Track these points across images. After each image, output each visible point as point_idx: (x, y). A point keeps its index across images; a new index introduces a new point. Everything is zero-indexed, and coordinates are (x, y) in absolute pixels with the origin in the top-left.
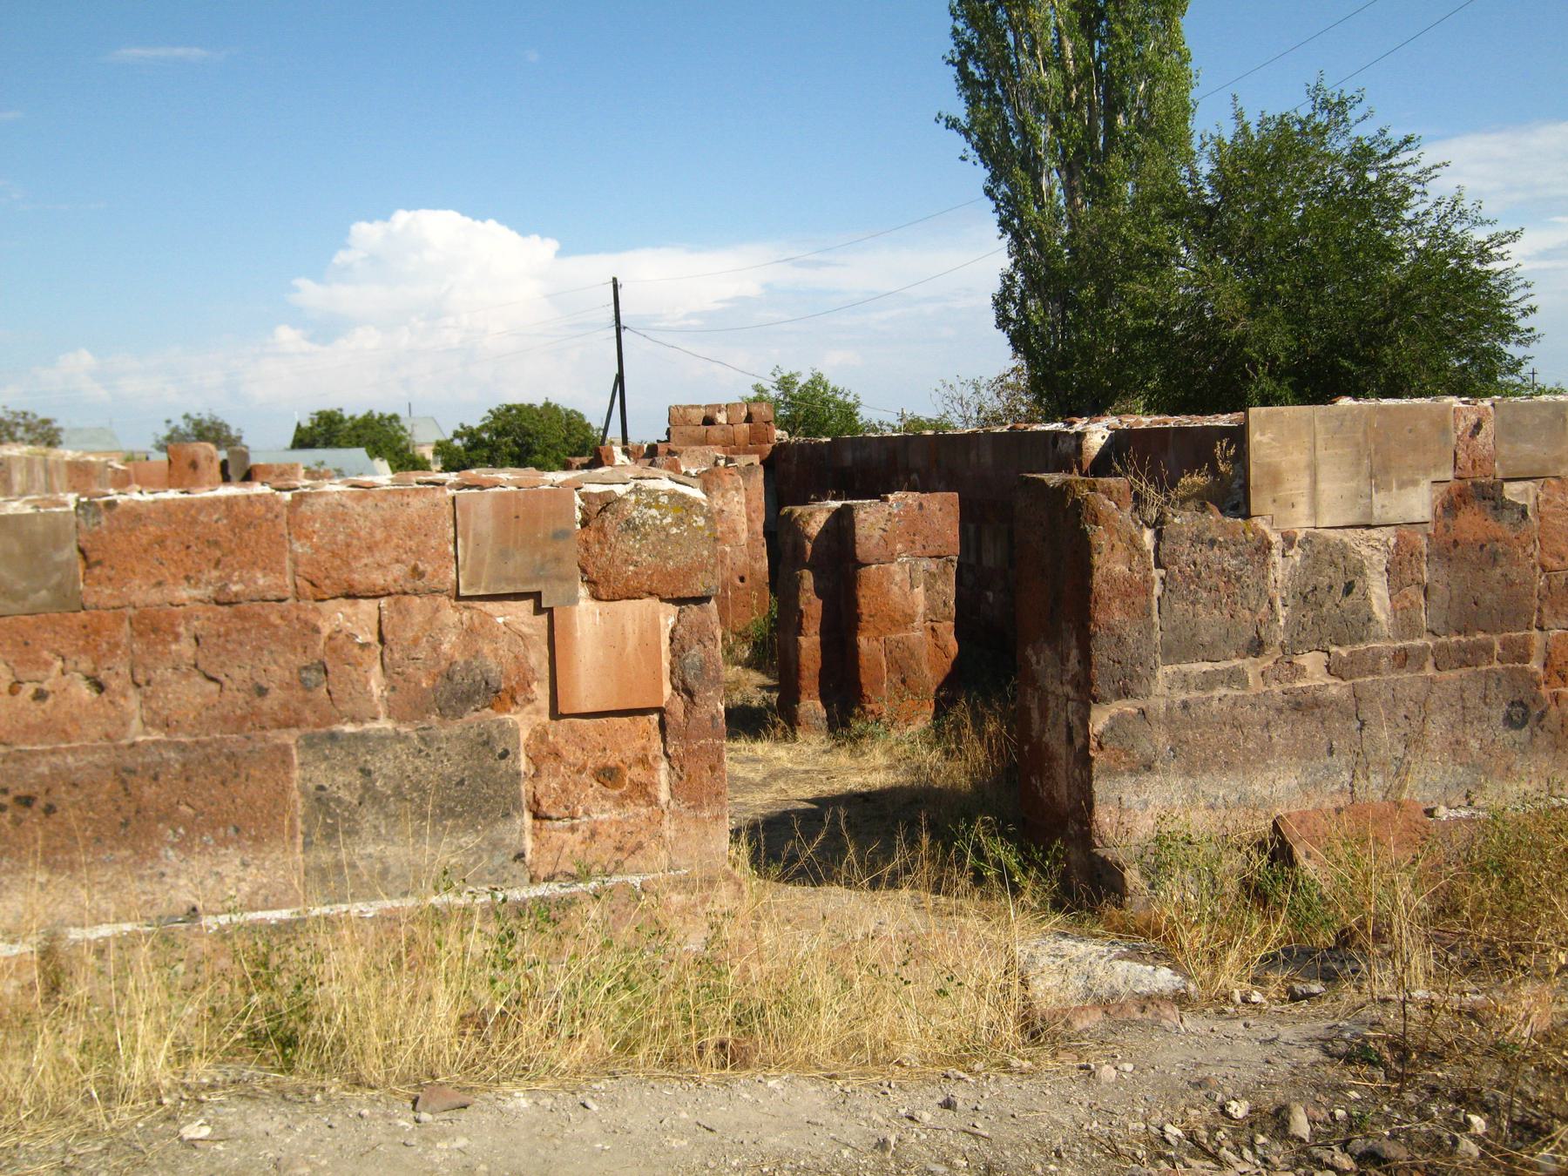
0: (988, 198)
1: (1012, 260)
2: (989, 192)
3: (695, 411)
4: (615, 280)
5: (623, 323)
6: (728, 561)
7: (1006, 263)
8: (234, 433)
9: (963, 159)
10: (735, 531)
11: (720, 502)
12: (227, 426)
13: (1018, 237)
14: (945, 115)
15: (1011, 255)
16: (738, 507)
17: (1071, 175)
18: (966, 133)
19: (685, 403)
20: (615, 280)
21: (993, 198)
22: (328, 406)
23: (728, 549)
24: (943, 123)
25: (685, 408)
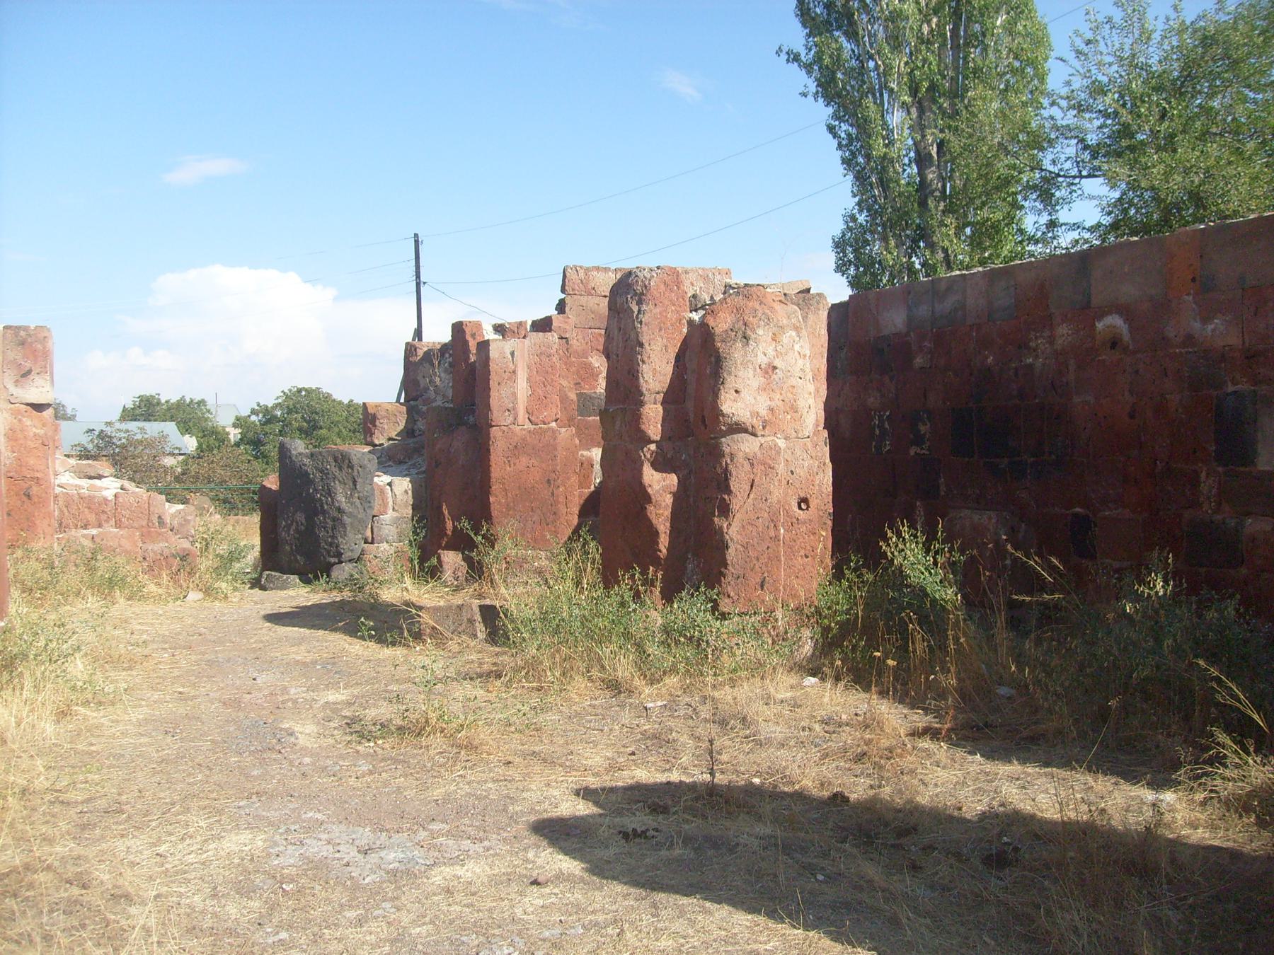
0: (831, 136)
1: (857, 199)
2: (831, 129)
3: (601, 275)
4: (416, 235)
5: (422, 279)
6: (781, 468)
7: (851, 203)
8: (69, 412)
9: (804, 95)
10: (794, 409)
11: (771, 352)
12: (63, 406)
13: (860, 178)
14: (785, 49)
15: (854, 196)
16: (800, 362)
17: (921, 111)
18: (808, 68)
19: (588, 264)
20: (416, 235)
21: (835, 136)
22: (148, 392)
23: (781, 443)
24: (784, 57)
25: (587, 270)
